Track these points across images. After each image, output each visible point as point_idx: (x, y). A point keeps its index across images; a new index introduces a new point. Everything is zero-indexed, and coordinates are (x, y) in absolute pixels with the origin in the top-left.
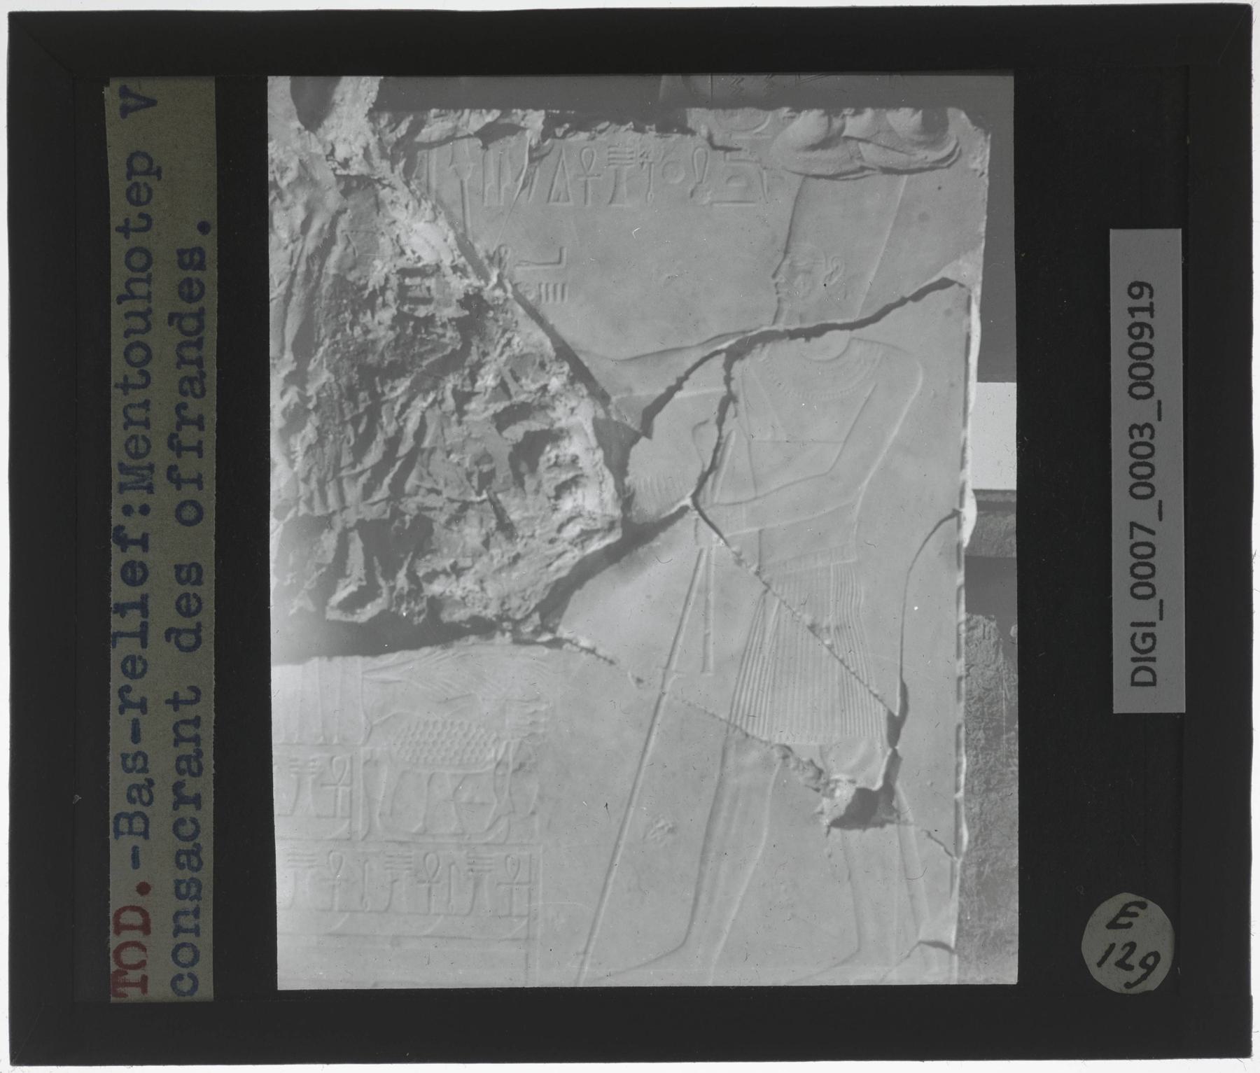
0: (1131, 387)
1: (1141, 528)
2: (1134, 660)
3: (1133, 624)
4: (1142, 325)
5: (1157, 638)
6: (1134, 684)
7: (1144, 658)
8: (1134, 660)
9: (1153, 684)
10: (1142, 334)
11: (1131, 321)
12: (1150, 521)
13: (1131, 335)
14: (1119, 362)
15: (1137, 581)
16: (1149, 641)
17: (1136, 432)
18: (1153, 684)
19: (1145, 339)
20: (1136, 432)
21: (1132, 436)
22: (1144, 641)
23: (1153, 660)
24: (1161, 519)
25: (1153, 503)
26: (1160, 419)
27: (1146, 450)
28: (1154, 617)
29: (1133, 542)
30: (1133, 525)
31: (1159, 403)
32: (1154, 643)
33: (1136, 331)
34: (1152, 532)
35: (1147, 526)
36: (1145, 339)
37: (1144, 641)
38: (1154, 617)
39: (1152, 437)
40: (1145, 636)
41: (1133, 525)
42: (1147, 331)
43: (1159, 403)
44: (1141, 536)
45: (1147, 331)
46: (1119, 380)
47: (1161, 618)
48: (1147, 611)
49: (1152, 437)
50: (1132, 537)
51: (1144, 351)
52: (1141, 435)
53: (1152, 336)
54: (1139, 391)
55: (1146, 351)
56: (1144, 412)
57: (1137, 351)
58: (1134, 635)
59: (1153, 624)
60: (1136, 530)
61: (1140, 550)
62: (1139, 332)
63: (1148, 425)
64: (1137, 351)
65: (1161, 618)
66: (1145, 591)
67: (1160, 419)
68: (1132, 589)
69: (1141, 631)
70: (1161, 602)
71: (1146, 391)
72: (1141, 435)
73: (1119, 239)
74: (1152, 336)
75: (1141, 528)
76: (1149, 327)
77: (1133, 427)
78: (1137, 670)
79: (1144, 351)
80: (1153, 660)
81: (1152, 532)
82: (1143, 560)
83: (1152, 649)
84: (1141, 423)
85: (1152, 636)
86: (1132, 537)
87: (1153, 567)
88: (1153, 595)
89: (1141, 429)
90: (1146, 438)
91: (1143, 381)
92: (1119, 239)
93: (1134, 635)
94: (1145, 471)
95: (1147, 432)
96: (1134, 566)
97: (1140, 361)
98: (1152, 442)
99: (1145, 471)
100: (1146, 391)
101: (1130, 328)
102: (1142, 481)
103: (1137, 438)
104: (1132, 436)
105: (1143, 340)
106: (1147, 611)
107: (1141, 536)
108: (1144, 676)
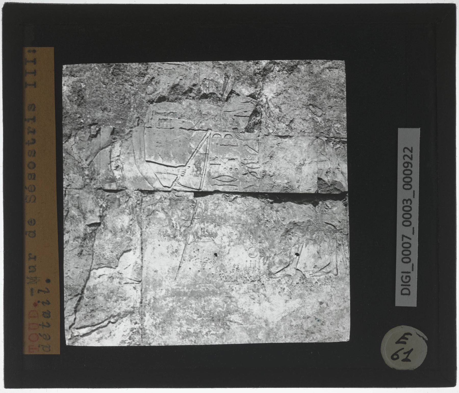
0: (404, 185)
1: (406, 237)
2: (402, 285)
3: (402, 272)
4: (408, 163)
5: (411, 278)
6: (402, 294)
7: (406, 285)
8: (402, 285)
9: (409, 294)
10: (408, 166)
11: (403, 161)
12: (410, 235)
13: (404, 166)
14: (400, 176)
15: (405, 176)
16: (408, 278)
17: (405, 202)
18: (409, 294)
19: (409, 168)
20: (405, 202)
21: (403, 204)
22: (406, 279)
23: (409, 285)
24: (413, 233)
25: (410, 228)
26: (414, 197)
27: (408, 209)
28: (410, 270)
29: (403, 242)
30: (403, 236)
31: (414, 191)
32: (410, 280)
33: (406, 165)
34: (410, 239)
35: (408, 236)
36: (409, 168)
37: (406, 279)
38: (410, 270)
39: (411, 204)
40: (406, 277)
41: (403, 236)
42: (410, 165)
43: (414, 191)
44: (406, 240)
45: (410, 165)
46: (400, 183)
47: (413, 270)
48: (408, 268)
49: (411, 204)
50: (403, 240)
51: (409, 172)
52: (407, 203)
53: (411, 167)
54: (406, 187)
55: (409, 172)
56: (408, 195)
57: (406, 172)
58: (402, 276)
59: (410, 273)
60: (404, 238)
61: (405, 245)
62: (407, 165)
63: (410, 200)
64: (406, 172)
65: (413, 270)
66: (407, 260)
67: (414, 197)
68: (403, 222)
69: (405, 275)
70: (413, 264)
71: (409, 187)
72: (407, 203)
73: (402, 132)
74: (411, 167)
75: (406, 237)
76: (411, 163)
77: (404, 200)
78: (403, 290)
79: (409, 172)
80: (409, 285)
81: (410, 239)
82: (406, 249)
83: (408, 282)
84: (407, 199)
85: (409, 277)
86: (403, 240)
87: (409, 251)
88: (410, 262)
89: (407, 201)
90: (409, 204)
91: (408, 183)
92: (402, 132)
93: (402, 276)
94: (408, 216)
95: (409, 202)
96: (403, 251)
97: (407, 176)
98: (411, 206)
99: (408, 216)
100: (409, 187)
101: (404, 164)
102: (407, 220)
103: (405, 204)
104: (403, 204)
105: (408, 168)
106: (408, 268)
107: (406, 240)
108: (405, 291)
